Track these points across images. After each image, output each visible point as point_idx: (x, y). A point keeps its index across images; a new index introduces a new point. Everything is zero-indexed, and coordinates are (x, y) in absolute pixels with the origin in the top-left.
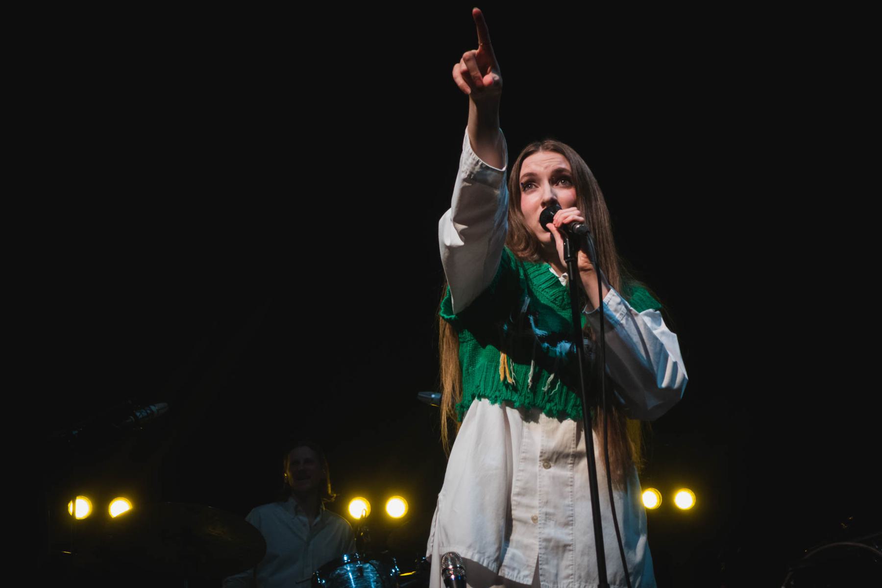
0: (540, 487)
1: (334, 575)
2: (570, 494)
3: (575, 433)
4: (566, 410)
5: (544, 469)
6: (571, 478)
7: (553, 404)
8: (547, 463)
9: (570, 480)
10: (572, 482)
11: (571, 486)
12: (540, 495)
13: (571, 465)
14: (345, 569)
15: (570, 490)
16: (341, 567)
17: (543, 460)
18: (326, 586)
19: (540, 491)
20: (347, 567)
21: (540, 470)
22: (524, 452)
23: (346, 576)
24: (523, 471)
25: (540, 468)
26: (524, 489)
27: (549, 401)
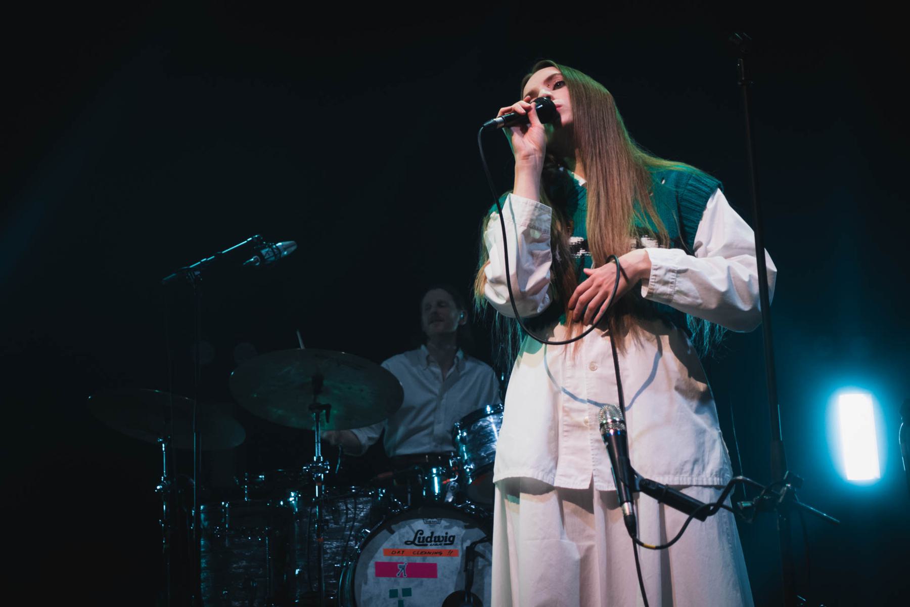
1: (477, 427)
14: (488, 421)
16: (483, 419)
18: (467, 439)
20: (490, 418)
23: (489, 428)
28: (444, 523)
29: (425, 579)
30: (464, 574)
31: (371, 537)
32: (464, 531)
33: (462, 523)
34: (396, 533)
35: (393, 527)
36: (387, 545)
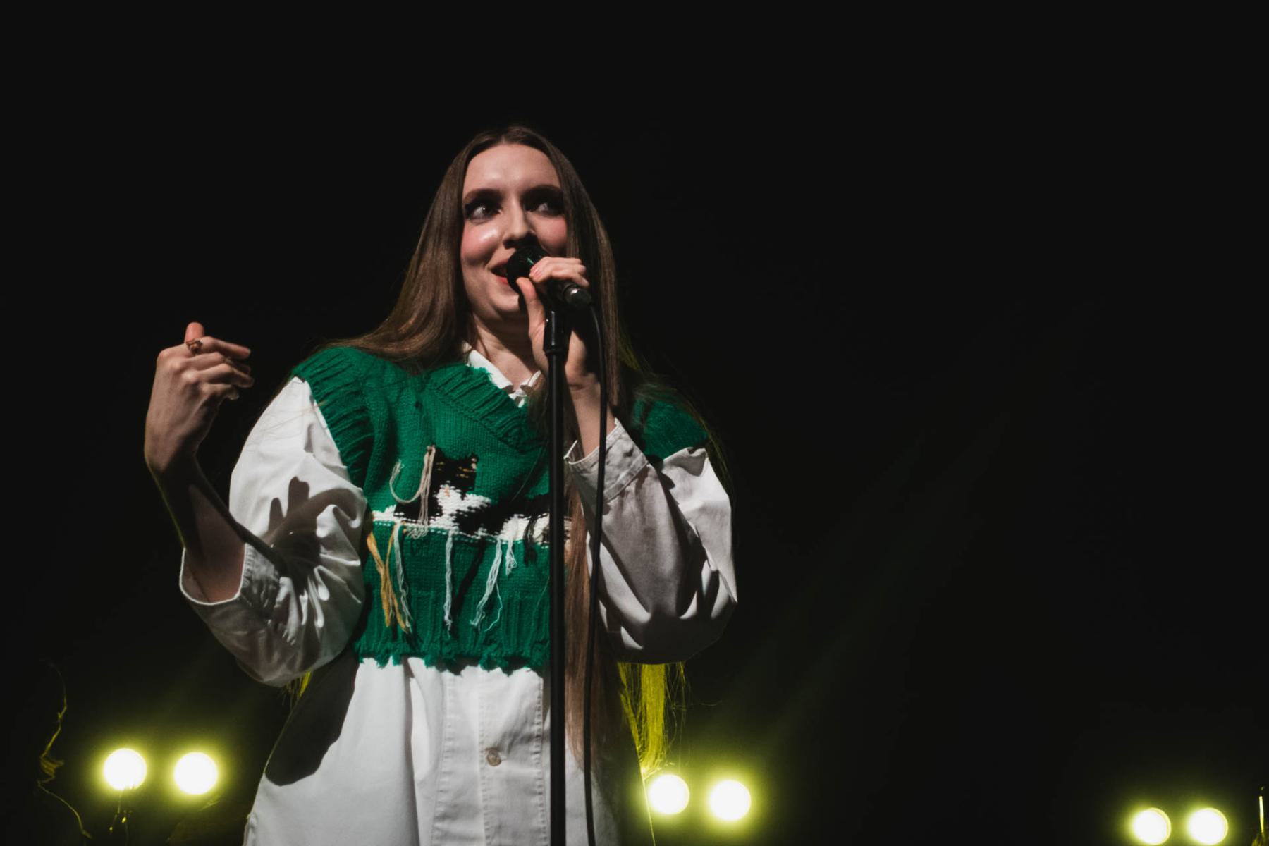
0: (485, 800)
2: (540, 809)
3: (542, 696)
4: (522, 652)
5: (489, 767)
6: (540, 779)
7: (494, 646)
8: (493, 754)
9: (538, 783)
10: (540, 786)
11: (540, 793)
12: (486, 814)
13: (537, 756)
15: (539, 802)
17: (487, 749)
19: (486, 808)
21: (482, 769)
22: (450, 739)
24: (449, 773)
25: (483, 765)
26: (455, 806)
27: (488, 641)
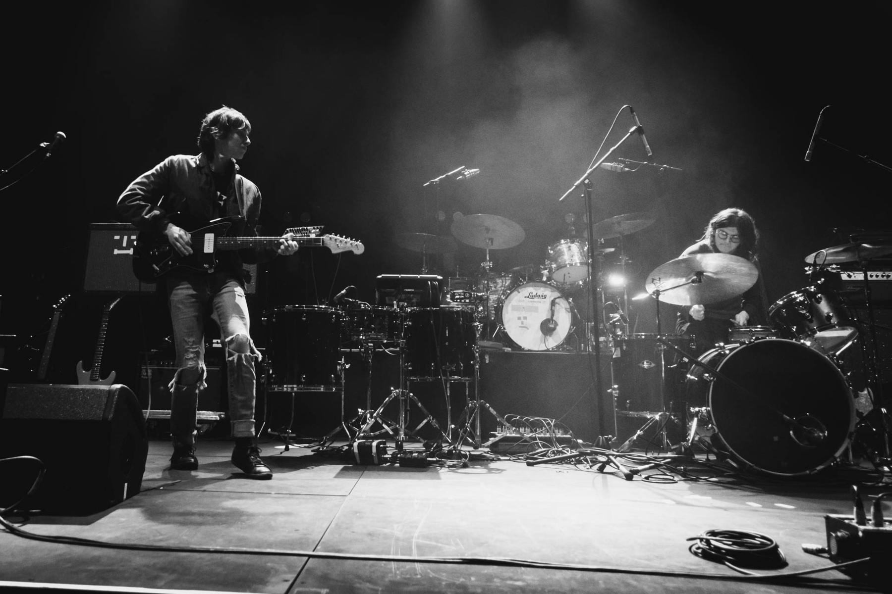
28: (542, 289)
29: (533, 313)
30: (550, 311)
31: (510, 294)
32: (551, 293)
33: (550, 290)
34: (521, 293)
35: (520, 290)
36: (516, 298)
